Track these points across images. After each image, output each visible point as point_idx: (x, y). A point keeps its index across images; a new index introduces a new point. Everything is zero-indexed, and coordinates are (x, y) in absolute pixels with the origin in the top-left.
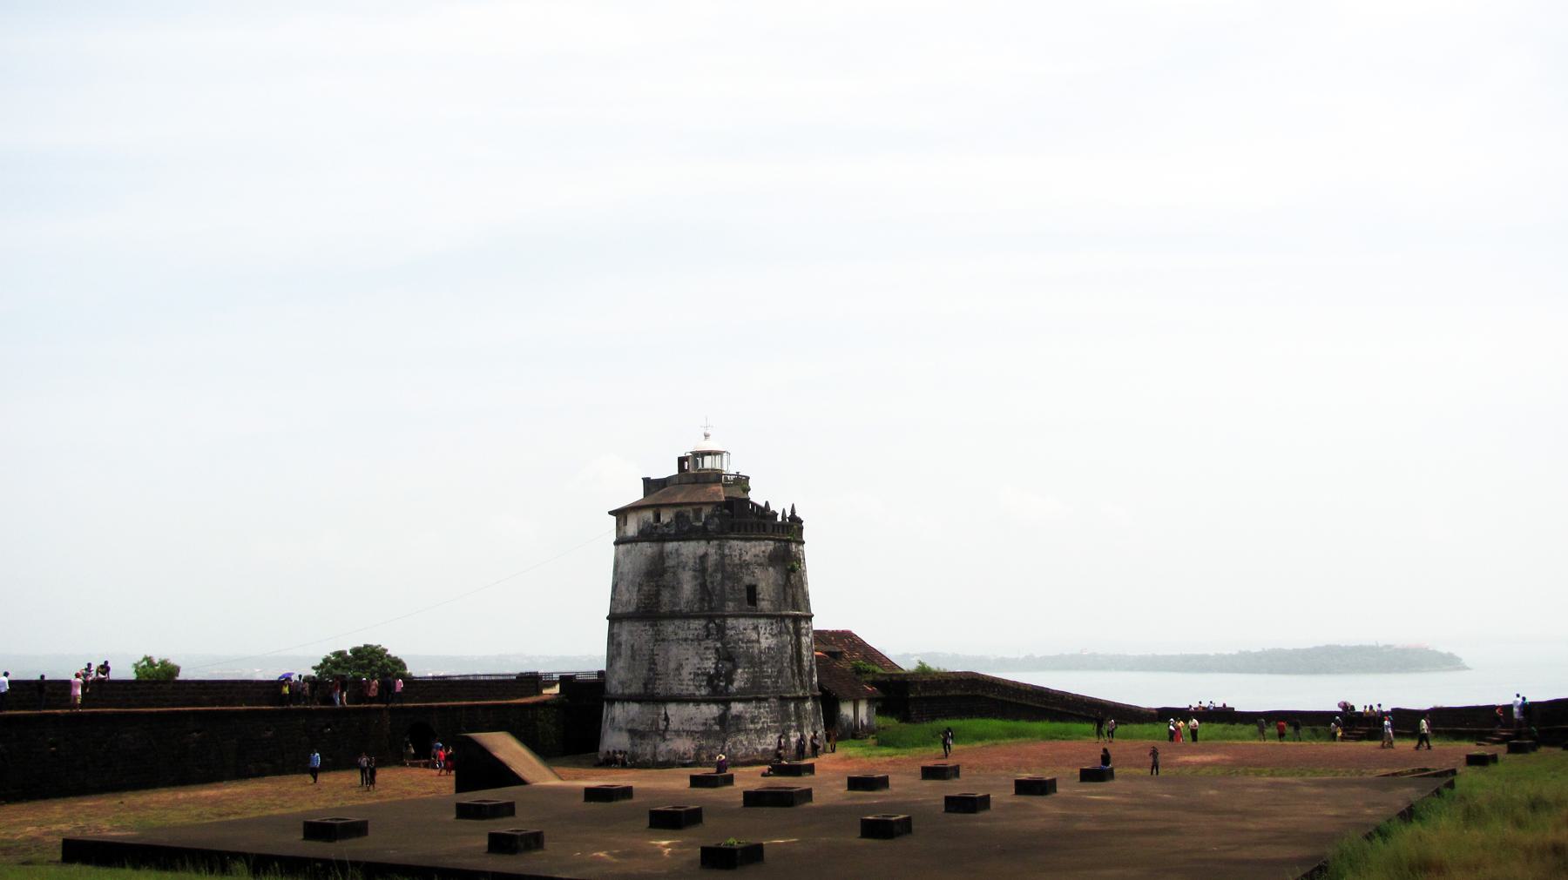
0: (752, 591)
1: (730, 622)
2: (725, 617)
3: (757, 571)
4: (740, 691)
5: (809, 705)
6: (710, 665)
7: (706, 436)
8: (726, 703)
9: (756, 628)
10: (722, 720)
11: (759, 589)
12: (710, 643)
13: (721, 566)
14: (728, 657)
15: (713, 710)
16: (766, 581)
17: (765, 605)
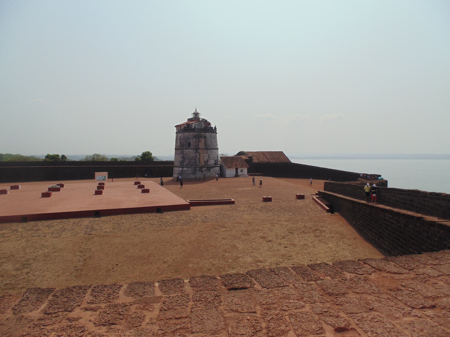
0: (189, 144)
1: (184, 150)
2: (183, 149)
3: (191, 140)
4: (186, 165)
5: (204, 169)
6: (181, 159)
7: (196, 110)
8: (183, 168)
9: (190, 152)
10: (182, 171)
11: (191, 143)
12: (181, 155)
13: (184, 138)
14: (183, 158)
15: (181, 169)
16: (193, 142)
17: (192, 147)
